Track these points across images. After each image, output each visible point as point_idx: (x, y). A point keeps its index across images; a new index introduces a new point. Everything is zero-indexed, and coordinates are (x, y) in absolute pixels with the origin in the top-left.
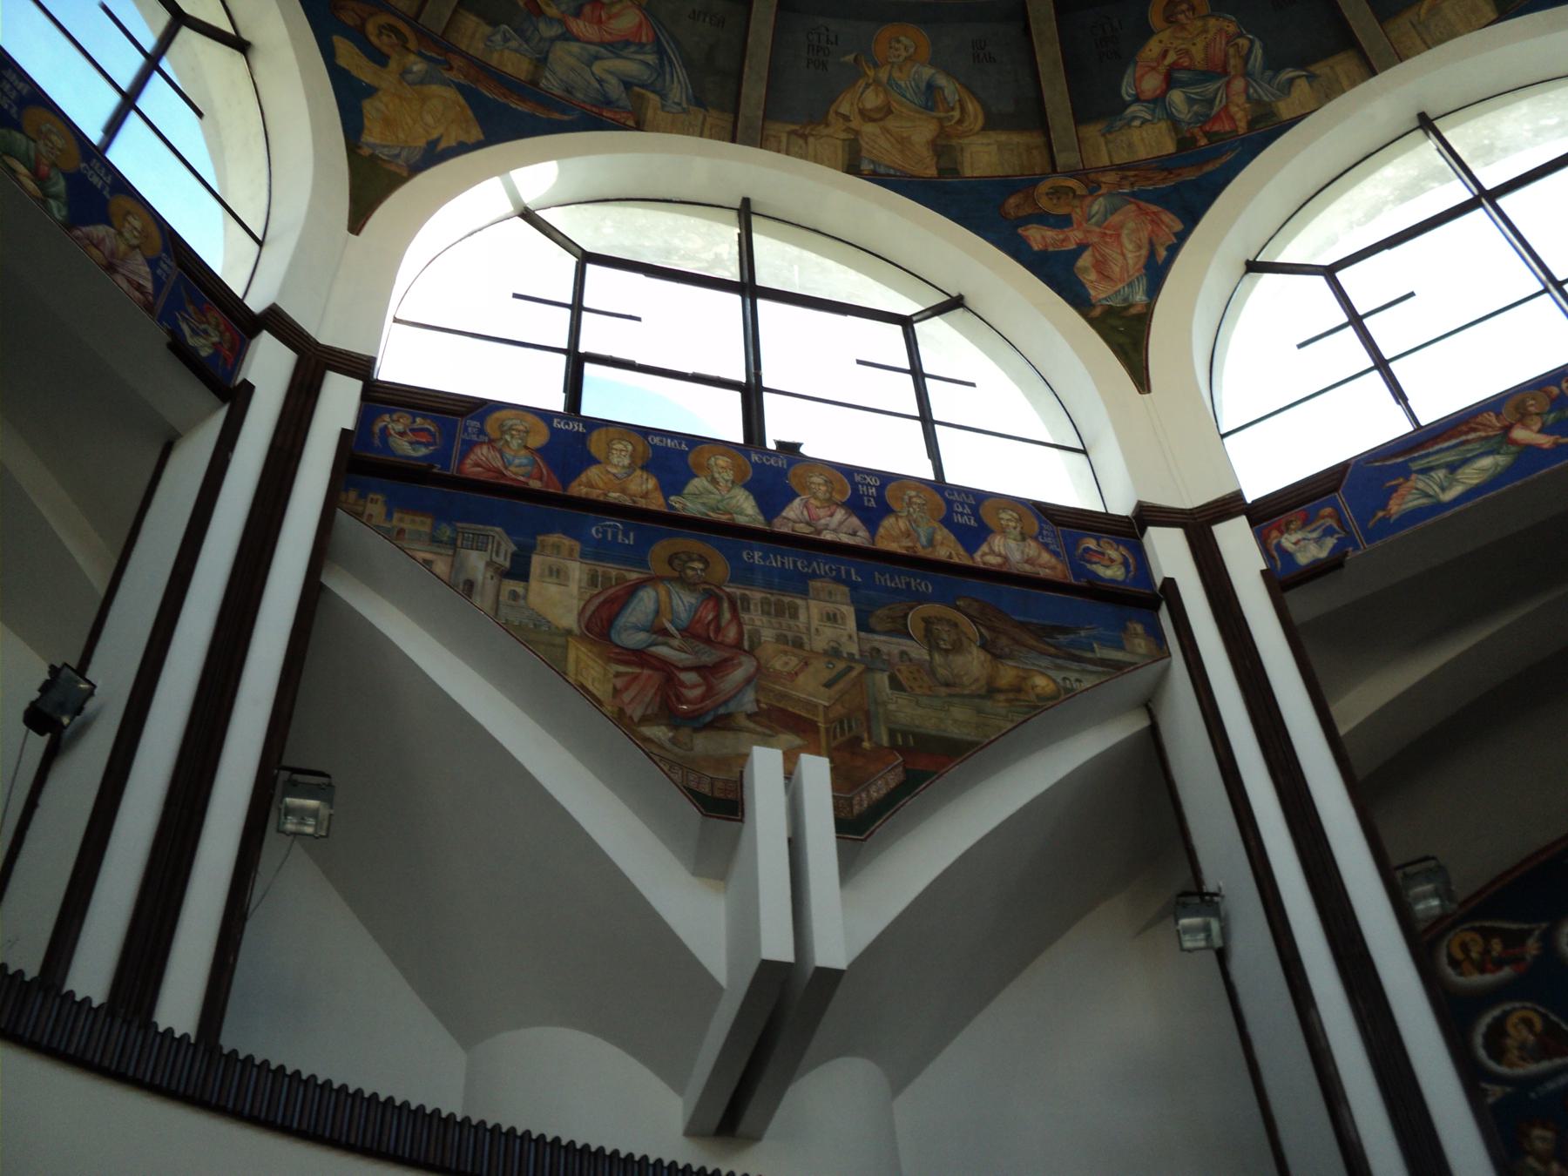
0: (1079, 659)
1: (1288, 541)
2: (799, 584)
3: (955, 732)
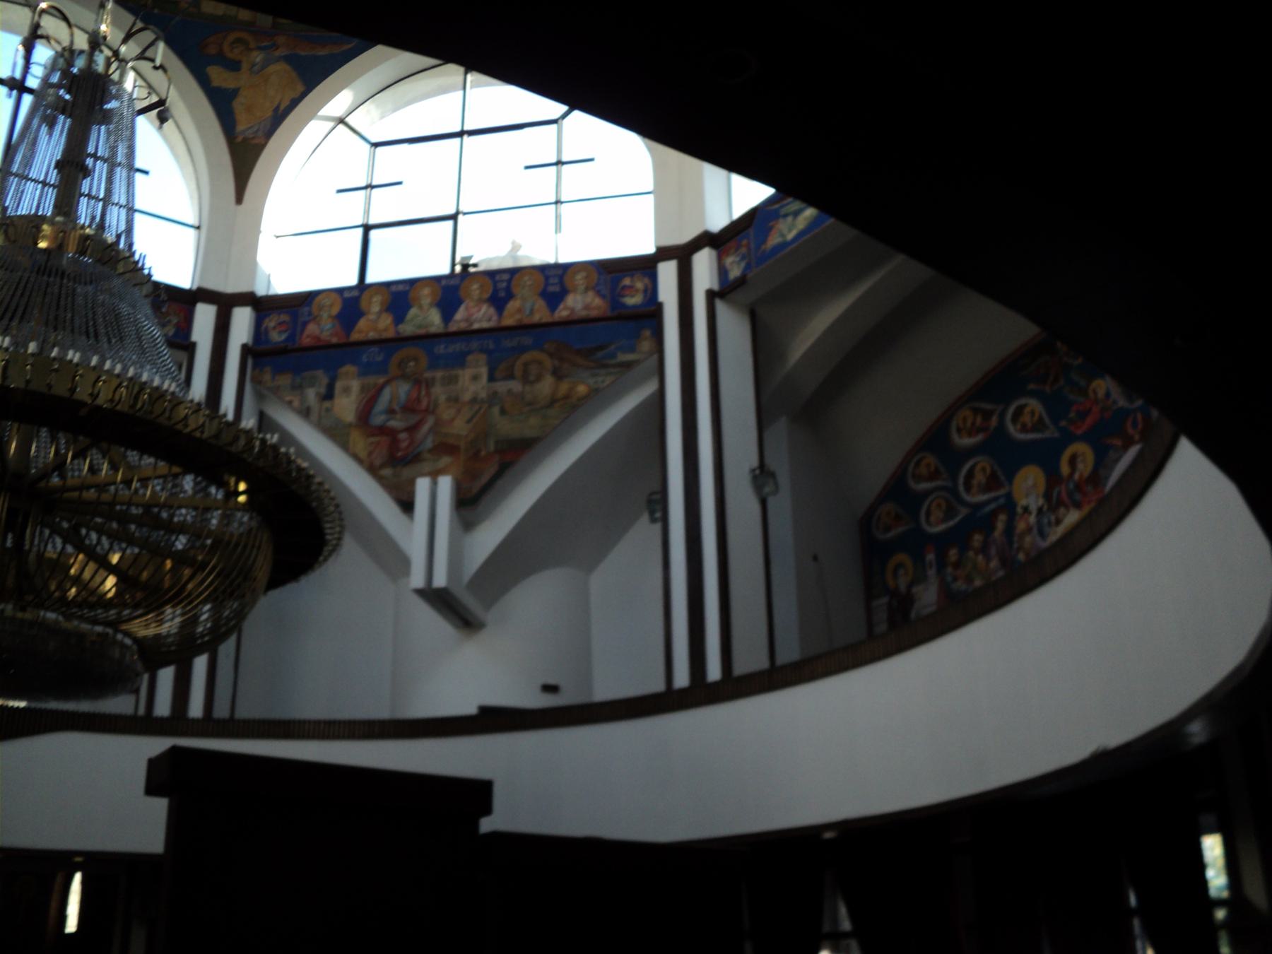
0: (605, 366)
1: (729, 260)
2: (459, 360)
3: (529, 433)
